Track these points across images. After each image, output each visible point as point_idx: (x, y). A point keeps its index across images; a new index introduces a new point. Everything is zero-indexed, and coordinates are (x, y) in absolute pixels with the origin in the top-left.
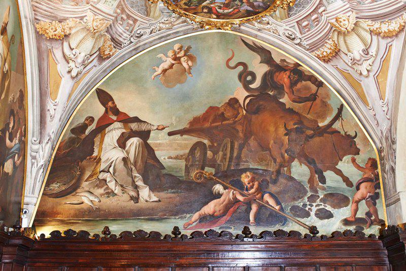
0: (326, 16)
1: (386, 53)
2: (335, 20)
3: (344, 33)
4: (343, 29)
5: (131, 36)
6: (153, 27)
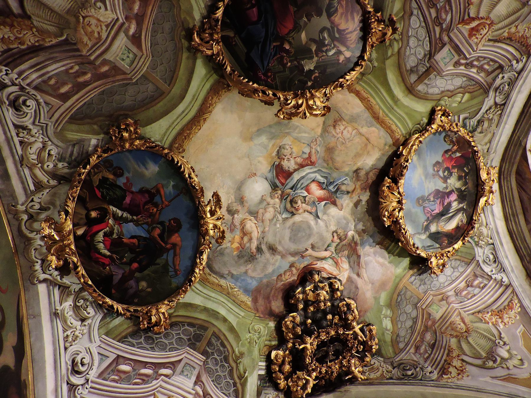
5: (22, 89)
6: (34, 131)
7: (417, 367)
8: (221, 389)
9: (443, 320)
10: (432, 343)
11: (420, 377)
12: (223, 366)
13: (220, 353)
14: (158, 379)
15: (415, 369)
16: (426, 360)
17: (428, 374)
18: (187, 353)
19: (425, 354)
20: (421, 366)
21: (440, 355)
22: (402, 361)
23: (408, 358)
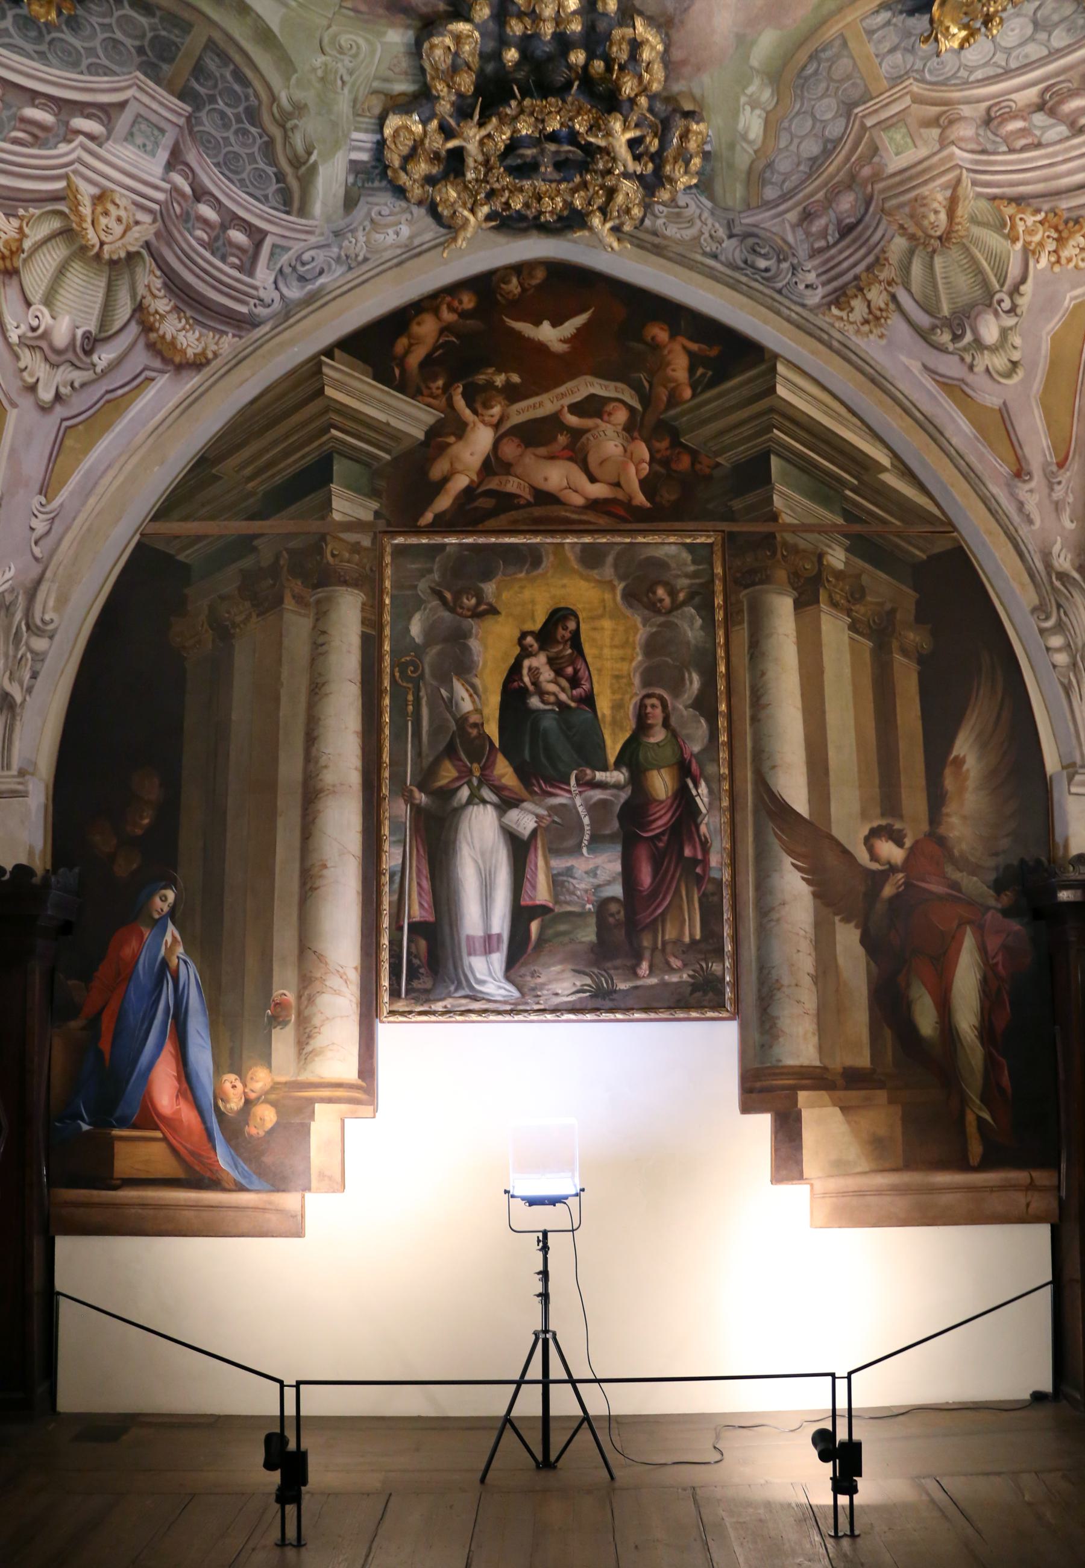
0: (80, 152)
1: (126, 389)
2: (95, 191)
3: (84, 249)
4: (92, 237)
7: (785, 260)
8: (242, 185)
9: (902, 183)
10: (848, 221)
11: (779, 285)
12: (245, 132)
13: (234, 99)
14: (70, 141)
15: (779, 261)
16: (814, 253)
17: (801, 287)
18: (140, 88)
19: (817, 239)
20: (795, 261)
21: (852, 260)
22: (755, 230)
23: (774, 230)
